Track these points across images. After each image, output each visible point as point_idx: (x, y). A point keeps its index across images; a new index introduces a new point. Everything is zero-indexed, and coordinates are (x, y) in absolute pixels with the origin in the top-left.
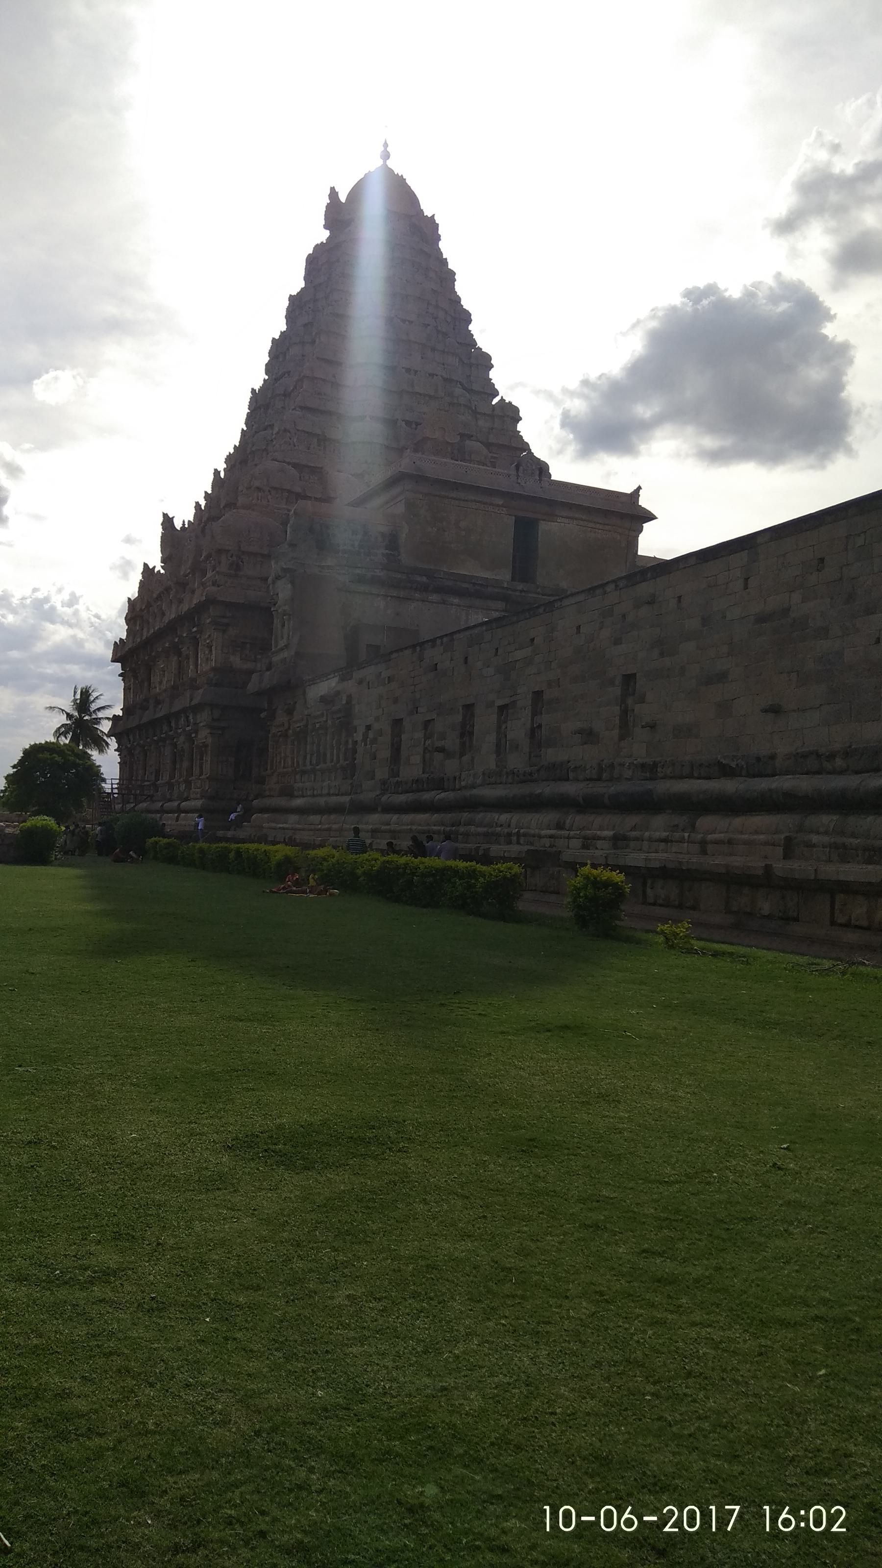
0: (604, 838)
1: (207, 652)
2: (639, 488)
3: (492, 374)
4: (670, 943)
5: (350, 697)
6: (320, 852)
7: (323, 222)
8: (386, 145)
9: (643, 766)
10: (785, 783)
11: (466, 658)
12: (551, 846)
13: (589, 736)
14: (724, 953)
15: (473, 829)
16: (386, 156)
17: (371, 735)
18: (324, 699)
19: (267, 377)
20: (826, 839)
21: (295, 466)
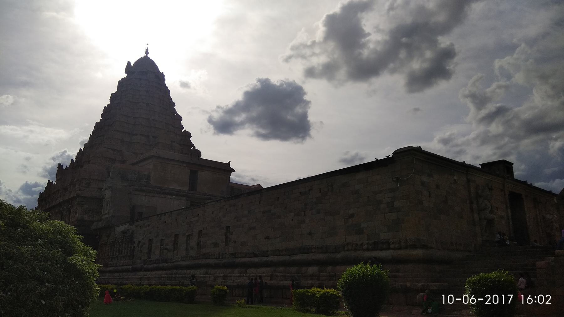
0: (221, 277)
1: (74, 214)
2: (230, 162)
3: (182, 122)
4: (240, 305)
5: (133, 231)
6: (126, 286)
7: (125, 71)
8: (147, 50)
9: (232, 254)
10: (270, 258)
11: (176, 220)
12: (204, 280)
13: (216, 245)
14: (253, 307)
15: (177, 275)
16: (147, 53)
17: (140, 244)
18: (124, 232)
19: (101, 118)
20: (281, 274)
21: (112, 149)
